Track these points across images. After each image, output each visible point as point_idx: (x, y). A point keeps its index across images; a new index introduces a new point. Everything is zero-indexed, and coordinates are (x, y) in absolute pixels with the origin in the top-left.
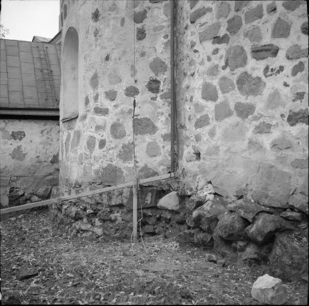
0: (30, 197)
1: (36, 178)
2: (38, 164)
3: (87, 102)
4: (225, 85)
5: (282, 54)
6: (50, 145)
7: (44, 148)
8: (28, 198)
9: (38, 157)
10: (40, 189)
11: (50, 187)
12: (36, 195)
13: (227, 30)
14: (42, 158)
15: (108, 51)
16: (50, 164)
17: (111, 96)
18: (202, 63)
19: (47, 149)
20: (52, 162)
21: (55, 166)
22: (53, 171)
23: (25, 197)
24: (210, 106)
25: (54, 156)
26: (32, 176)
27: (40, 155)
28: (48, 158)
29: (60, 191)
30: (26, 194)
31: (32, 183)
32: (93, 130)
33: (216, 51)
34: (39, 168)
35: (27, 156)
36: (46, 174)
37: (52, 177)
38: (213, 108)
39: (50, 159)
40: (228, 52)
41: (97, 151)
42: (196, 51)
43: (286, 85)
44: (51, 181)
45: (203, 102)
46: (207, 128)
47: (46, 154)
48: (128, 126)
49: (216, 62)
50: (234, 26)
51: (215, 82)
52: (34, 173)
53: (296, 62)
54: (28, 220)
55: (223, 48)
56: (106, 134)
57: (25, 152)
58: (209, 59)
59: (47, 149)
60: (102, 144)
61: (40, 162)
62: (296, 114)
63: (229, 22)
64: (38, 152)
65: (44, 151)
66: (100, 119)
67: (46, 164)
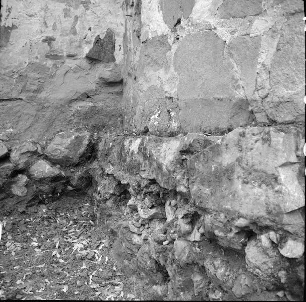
0: (28, 165)
1: (42, 107)
2: (49, 63)
6: (87, 8)
7: (66, 13)
8: (21, 166)
9: (49, 40)
10: (57, 139)
11: (86, 134)
12: (46, 158)
14: (62, 45)
16: (85, 64)
19: (77, 18)
20: (92, 59)
21: (104, 71)
22: (93, 87)
23: (11, 165)
25: (98, 40)
26: (31, 99)
27: (57, 35)
28: (80, 47)
29: (227, 159)
30: (14, 155)
31: (31, 121)
34: (52, 77)
35: (13, 33)
36: (72, 96)
37: (87, 104)
39: (86, 49)
44: (86, 116)
47: (75, 33)
52: (37, 91)
54: (27, 240)
57: (9, 23)
59: (77, 18)
61: (54, 56)
64: (50, 24)
65: (67, 24)
67: (71, 64)
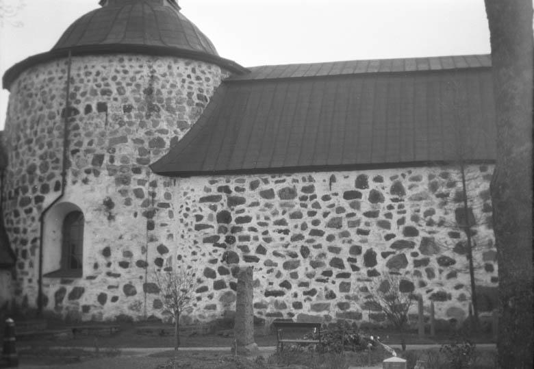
3: (96, 266)
4: (223, 271)
5: (261, 263)
13: (226, 241)
15: (122, 232)
17: (124, 265)
18: (204, 255)
24: (209, 283)
32: (106, 288)
33: (215, 251)
38: (213, 283)
40: (225, 253)
41: (109, 303)
42: (197, 247)
43: (263, 277)
45: (204, 278)
46: (206, 293)
48: (139, 288)
49: (216, 257)
50: (230, 240)
51: (215, 268)
53: (270, 268)
55: (221, 251)
56: (120, 292)
58: (210, 254)
60: (115, 299)
62: (269, 292)
63: (226, 237)
66: (112, 281)
